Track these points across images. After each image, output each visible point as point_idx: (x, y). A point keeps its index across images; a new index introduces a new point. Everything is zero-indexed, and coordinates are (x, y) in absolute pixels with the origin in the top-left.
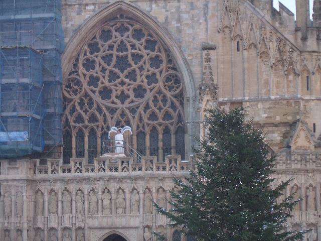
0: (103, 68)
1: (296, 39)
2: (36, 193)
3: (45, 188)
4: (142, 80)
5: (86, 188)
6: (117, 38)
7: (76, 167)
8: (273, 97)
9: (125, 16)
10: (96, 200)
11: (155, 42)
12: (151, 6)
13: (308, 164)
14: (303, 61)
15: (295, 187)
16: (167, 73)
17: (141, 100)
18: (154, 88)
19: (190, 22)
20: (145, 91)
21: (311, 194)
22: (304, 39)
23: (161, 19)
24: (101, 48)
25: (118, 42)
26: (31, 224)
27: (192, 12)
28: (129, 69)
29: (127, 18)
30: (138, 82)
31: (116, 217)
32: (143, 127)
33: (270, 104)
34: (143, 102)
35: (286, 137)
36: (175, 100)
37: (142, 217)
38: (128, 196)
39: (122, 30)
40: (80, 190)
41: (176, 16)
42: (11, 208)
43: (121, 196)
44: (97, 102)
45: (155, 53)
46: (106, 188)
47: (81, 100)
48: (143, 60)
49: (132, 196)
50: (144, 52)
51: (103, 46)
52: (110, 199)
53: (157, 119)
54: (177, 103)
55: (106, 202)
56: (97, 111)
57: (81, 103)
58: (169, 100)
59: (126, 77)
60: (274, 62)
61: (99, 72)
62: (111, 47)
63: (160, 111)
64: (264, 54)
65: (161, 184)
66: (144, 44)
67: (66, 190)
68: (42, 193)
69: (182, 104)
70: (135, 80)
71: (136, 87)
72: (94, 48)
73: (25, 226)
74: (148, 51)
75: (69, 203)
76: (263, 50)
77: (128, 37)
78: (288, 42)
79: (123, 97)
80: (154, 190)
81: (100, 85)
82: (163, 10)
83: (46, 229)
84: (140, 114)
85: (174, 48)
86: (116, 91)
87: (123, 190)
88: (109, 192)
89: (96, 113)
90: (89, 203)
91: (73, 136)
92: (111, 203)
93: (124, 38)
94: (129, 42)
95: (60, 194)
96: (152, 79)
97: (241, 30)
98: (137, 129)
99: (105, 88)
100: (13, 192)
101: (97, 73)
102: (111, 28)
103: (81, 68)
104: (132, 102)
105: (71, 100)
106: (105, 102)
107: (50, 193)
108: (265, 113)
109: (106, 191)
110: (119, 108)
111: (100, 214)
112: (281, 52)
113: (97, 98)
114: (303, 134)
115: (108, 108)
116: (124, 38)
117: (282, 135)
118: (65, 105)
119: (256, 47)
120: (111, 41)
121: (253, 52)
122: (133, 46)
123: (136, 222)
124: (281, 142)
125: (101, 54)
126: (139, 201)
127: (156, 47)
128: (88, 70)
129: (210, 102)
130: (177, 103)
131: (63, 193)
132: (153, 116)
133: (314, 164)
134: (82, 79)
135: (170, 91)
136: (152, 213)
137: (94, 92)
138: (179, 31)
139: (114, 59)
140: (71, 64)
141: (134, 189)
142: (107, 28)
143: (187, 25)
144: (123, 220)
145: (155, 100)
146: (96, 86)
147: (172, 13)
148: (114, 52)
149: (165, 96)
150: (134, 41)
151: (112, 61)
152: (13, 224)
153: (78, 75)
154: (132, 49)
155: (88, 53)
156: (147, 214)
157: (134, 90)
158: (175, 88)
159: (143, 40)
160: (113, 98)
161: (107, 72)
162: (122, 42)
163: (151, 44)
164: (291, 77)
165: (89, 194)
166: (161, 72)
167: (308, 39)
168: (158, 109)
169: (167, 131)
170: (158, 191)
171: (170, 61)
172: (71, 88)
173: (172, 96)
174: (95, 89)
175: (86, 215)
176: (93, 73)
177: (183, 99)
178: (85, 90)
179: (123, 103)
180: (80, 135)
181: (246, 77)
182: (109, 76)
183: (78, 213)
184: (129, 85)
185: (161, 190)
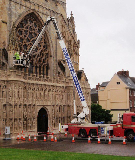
6: (29, 24)
9: (31, 16)
18: (41, 48)
25: (30, 26)
34: (37, 54)
55: (42, 94)
62: (27, 27)
90: (36, 94)
93: (32, 25)
95: (27, 89)
123: (49, 104)
131: (28, 89)
137: (22, 45)
138: (50, 29)
146: (22, 43)
158: (46, 51)
159: (37, 28)
161: (26, 37)
166: (42, 43)
171: (45, 39)
174: (22, 44)
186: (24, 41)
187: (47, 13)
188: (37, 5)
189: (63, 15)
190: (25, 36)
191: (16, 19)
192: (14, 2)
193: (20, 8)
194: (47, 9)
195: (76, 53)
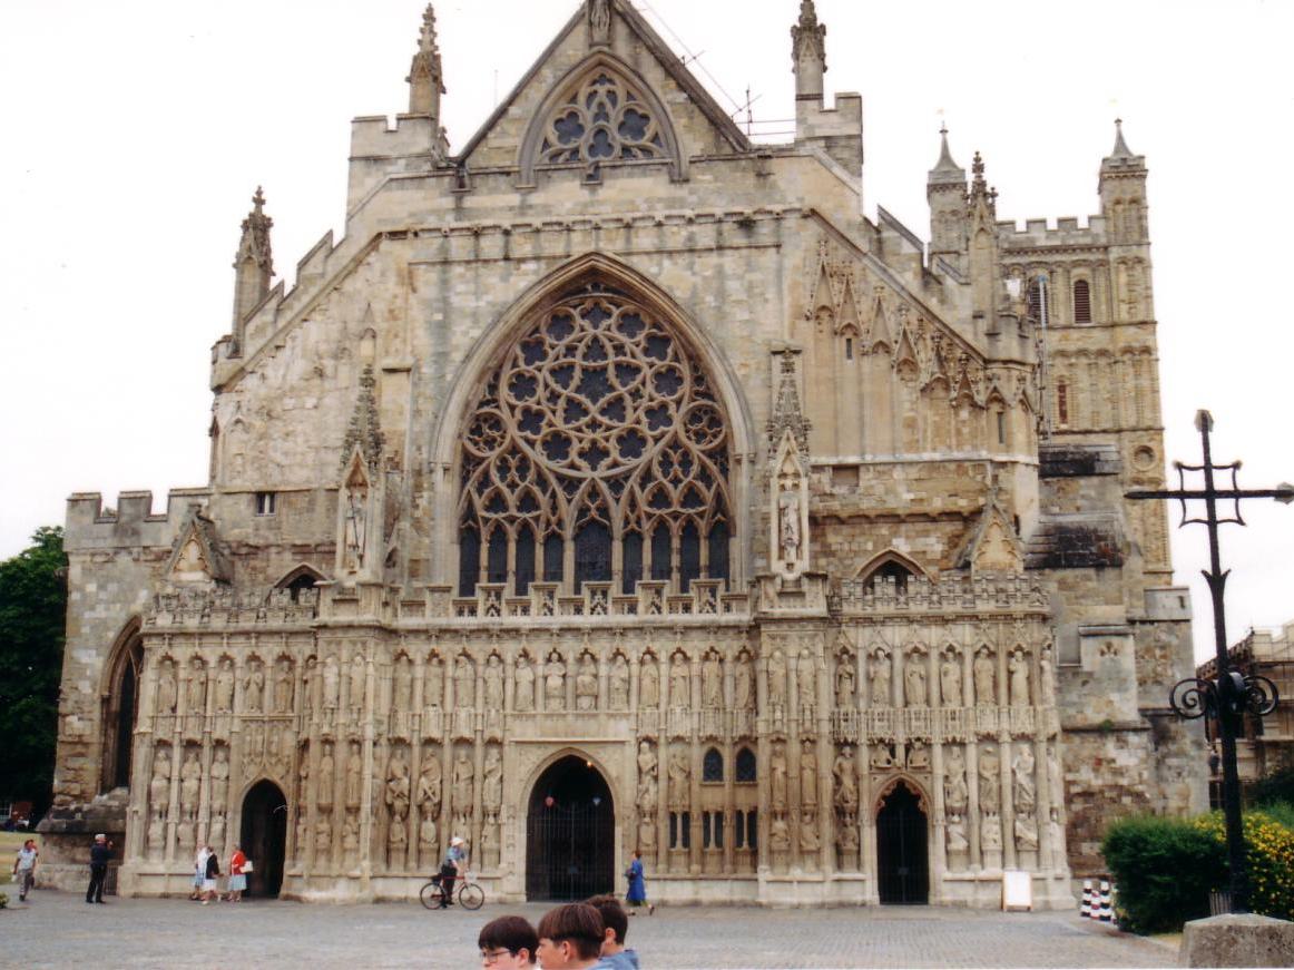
0: (552, 392)
1: (976, 334)
2: (397, 659)
4: (635, 416)
5: (510, 649)
6: (584, 329)
7: (490, 603)
8: (926, 456)
9: (602, 286)
10: (532, 678)
11: (666, 341)
12: (660, 265)
13: (1012, 601)
14: (990, 379)
15: (985, 651)
16: (692, 405)
17: (632, 462)
18: (663, 435)
19: (745, 298)
20: (643, 441)
21: (1021, 669)
22: (992, 335)
23: (680, 294)
24: (549, 350)
25: (587, 340)
26: (384, 728)
27: (749, 276)
28: (609, 396)
29: (606, 290)
30: (628, 423)
31: (577, 716)
32: (638, 522)
33: (920, 470)
35: (956, 546)
36: (709, 462)
37: (633, 718)
38: (603, 670)
39: (596, 314)
40: (494, 654)
41: (715, 284)
42: (339, 691)
43: (591, 668)
44: (536, 465)
45: (667, 362)
46: (555, 650)
47: (504, 460)
48: (639, 378)
49: (614, 668)
50: (642, 361)
51: (555, 346)
52: (564, 676)
53: (669, 505)
54: (714, 468)
55: (555, 682)
56: (538, 484)
57: (503, 468)
58: (696, 461)
59: (603, 412)
60: (927, 381)
61: (543, 401)
62: (571, 350)
63: (676, 487)
64: (908, 365)
65: (678, 644)
66: (643, 344)
67: (465, 654)
68: (411, 662)
69: (725, 471)
70: (622, 419)
71: (624, 433)
72: (534, 350)
73: (370, 733)
74: (653, 359)
75: (470, 684)
76: (904, 355)
77: (607, 329)
78: (957, 341)
79: (594, 454)
80: (663, 657)
81: (545, 430)
82: (689, 273)
83: (415, 742)
84: (632, 493)
85: (711, 352)
86: (581, 442)
87: (593, 657)
88: (560, 659)
89: (536, 490)
90: (516, 684)
91: (483, 540)
92: (564, 684)
94: (611, 341)
95: (450, 662)
96: (658, 415)
97: (855, 315)
98: (625, 527)
99: (556, 435)
100: (345, 655)
101: (539, 403)
102: (572, 310)
103: (504, 393)
104: (615, 464)
105: (482, 460)
106: (553, 465)
107: (429, 661)
108: (909, 491)
109: (555, 656)
110: (585, 479)
111: (540, 709)
112: (941, 361)
113: (537, 456)
114: (996, 535)
115: (561, 478)
116: (599, 332)
117: (945, 540)
118: (468, 472)
119: (888, 351)
120: (572, 337)
121: (882, 361)
122: (619, 349)
123: (622, 730)
124: (945, 556)
125: (548, 364)
126: (628, 681)
127: (670, 351)
128: (519, 397)
129: (793, 456)
130: (714, 468)
131: (457, 662)
132: (660, 498)
133: (1027, 602)
134: (505, 414)
135: (698, 442)
136: (657, 706)
137: (531, 443)
138: (721, 316)
139: (577, 374)
140: (484, 386)
141: (618, 653)
142: (563, 309)
143: (739, 302)
144: (592, 725)
145: (666, 463)
146: (537, 431)
147: (705, 278)
148: (578, 360)
149: (686, 454)
150: (622, 338)
151: (572, 378)
152: (340, 728)
153: (497, 407)
154: (617, 355)
155: (521, 363)
156: (648, 711)
157: (620, 439)
159: (641, 337)
160: (573, 455)
162: (595, 339)
163: (657, 345)
164: (964, 414)
165: (516, 664)
166: (679, 402)
167: (1002, 337)
168: (671, 482)
169: (690, 531)
170: (672, 659)
171: (699, 380)
172: (481, 435)
173: (703, 452)
174: (534, 437)
175: (509, 710)
176: (531, 402)
177: (727, 460)
178: (513, 439)
179: (594, 468)
180: (499, 536)
181: (867, 412)
182: (565, 411)
183: (490, 707)
184: (609, 428)
185: (679, 656)
186: (543, 424)
187: (691, 238)
188: (612, 225)
189: (826, 208)
190: (554, 397)
191: (476, 333)
192: (468, 262)
193: (505, 278)
194: (690, 221)
195: (970, 397)
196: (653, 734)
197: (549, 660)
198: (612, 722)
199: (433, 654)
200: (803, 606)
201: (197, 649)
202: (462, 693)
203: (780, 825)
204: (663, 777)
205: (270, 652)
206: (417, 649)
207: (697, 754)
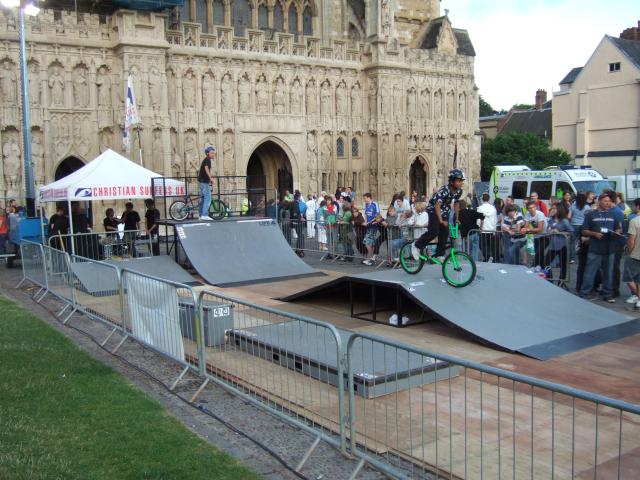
3: (181, 66)
5: (237, 71)
7: (221, 40)
43: (281, 87)
67: (210, 73)
95: (199, 77)
123: (296, 125)
131: (203, 77)
185: (326, 83)
196: (314, 128)
197: (258, 81)
198: (292, 121)
199: (190, 71)
200: (398, 61)
201: (8, 53)
202: (209, 99)
203: (387, 179)
204: (319, 154)
205: (69, 60)
206: (181, 66)
207: (335, 138)
